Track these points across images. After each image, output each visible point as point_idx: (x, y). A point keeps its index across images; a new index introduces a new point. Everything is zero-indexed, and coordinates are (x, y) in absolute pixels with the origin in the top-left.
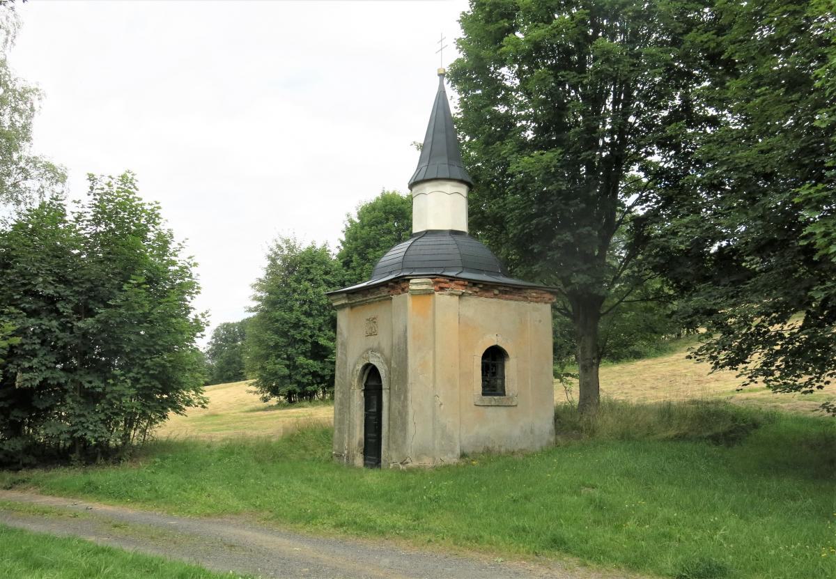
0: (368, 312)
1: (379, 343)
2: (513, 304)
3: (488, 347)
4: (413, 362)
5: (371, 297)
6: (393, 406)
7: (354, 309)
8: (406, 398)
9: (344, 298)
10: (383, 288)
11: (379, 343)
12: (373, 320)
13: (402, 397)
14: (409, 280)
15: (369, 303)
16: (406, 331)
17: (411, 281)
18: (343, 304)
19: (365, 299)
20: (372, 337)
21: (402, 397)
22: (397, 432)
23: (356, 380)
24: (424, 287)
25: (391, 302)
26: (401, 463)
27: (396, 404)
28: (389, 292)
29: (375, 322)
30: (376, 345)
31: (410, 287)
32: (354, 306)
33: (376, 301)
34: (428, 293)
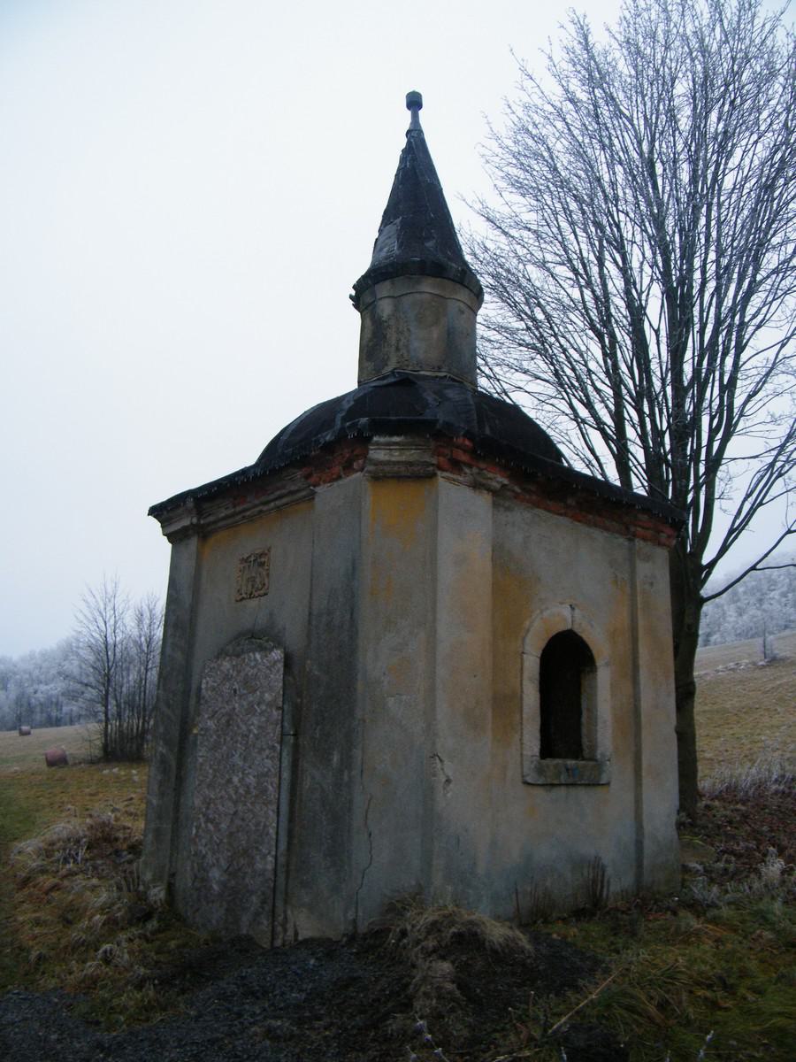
0: (249, 541)
1: (271, 614)
2: (600, 536)
4: (376, 660)
5: (257, 502)
6: (307, 783)
7: (212, 540)
8: (347, 762)
11: (271, 614)
12: (259, 561)
13: (336, 758)
15: (251, 519)
16: (353, 570)
18: (185, 529)
19: (239, 509)
20: (253, 603)
21: (336, 758)
28: (308, 477)
29: (262, 564)
34: (421, 476)
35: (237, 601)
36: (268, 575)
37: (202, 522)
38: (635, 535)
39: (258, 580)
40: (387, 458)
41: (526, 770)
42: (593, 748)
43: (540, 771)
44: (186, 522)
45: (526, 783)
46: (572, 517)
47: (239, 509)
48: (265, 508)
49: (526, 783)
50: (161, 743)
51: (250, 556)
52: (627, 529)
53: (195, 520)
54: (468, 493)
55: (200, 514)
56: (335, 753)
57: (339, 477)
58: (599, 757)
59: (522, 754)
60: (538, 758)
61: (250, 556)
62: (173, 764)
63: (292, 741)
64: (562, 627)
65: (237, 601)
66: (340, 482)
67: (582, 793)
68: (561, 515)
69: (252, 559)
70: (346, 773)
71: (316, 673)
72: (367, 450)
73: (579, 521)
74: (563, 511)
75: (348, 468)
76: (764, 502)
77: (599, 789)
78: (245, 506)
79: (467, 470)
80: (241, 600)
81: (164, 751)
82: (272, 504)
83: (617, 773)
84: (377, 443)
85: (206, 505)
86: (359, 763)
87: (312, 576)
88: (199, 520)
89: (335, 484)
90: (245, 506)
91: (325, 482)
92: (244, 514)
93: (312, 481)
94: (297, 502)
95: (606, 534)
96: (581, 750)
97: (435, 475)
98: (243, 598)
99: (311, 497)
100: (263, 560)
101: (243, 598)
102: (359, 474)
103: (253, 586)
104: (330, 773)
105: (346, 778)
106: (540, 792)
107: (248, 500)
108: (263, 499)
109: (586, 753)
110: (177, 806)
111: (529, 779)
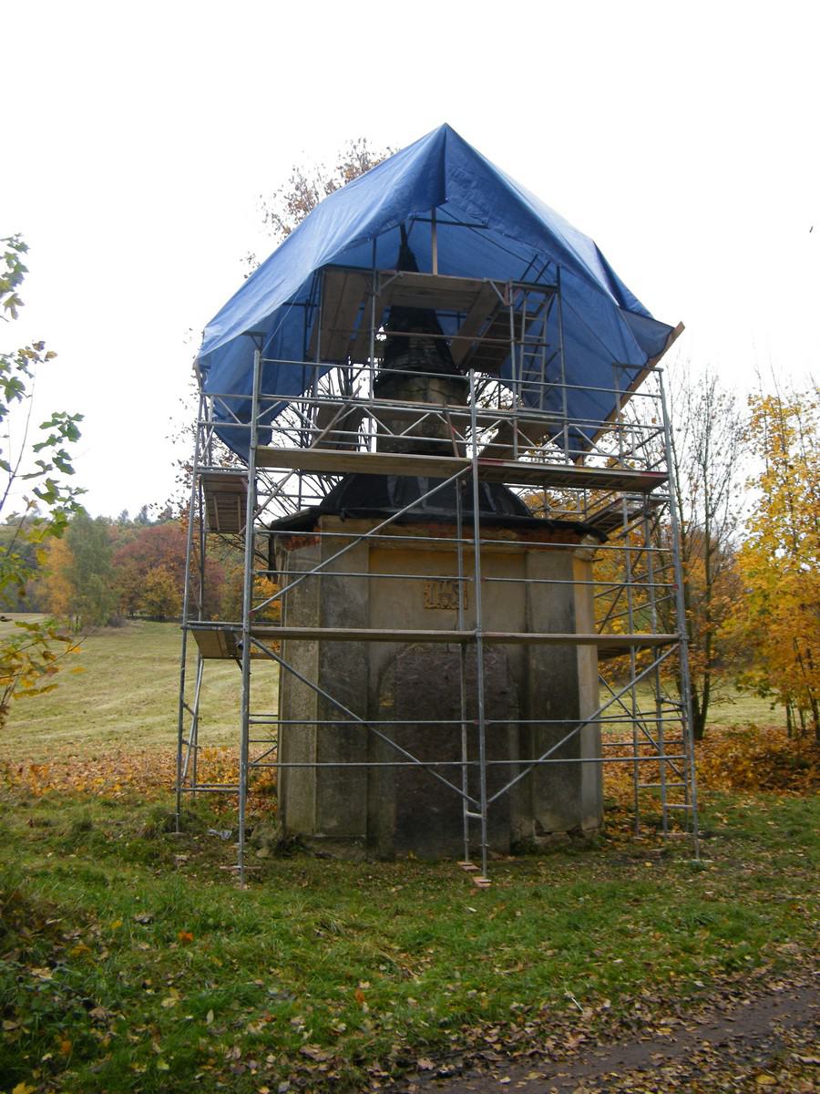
35: (427, 608)
65: (427, 608)
71: (542, 669)
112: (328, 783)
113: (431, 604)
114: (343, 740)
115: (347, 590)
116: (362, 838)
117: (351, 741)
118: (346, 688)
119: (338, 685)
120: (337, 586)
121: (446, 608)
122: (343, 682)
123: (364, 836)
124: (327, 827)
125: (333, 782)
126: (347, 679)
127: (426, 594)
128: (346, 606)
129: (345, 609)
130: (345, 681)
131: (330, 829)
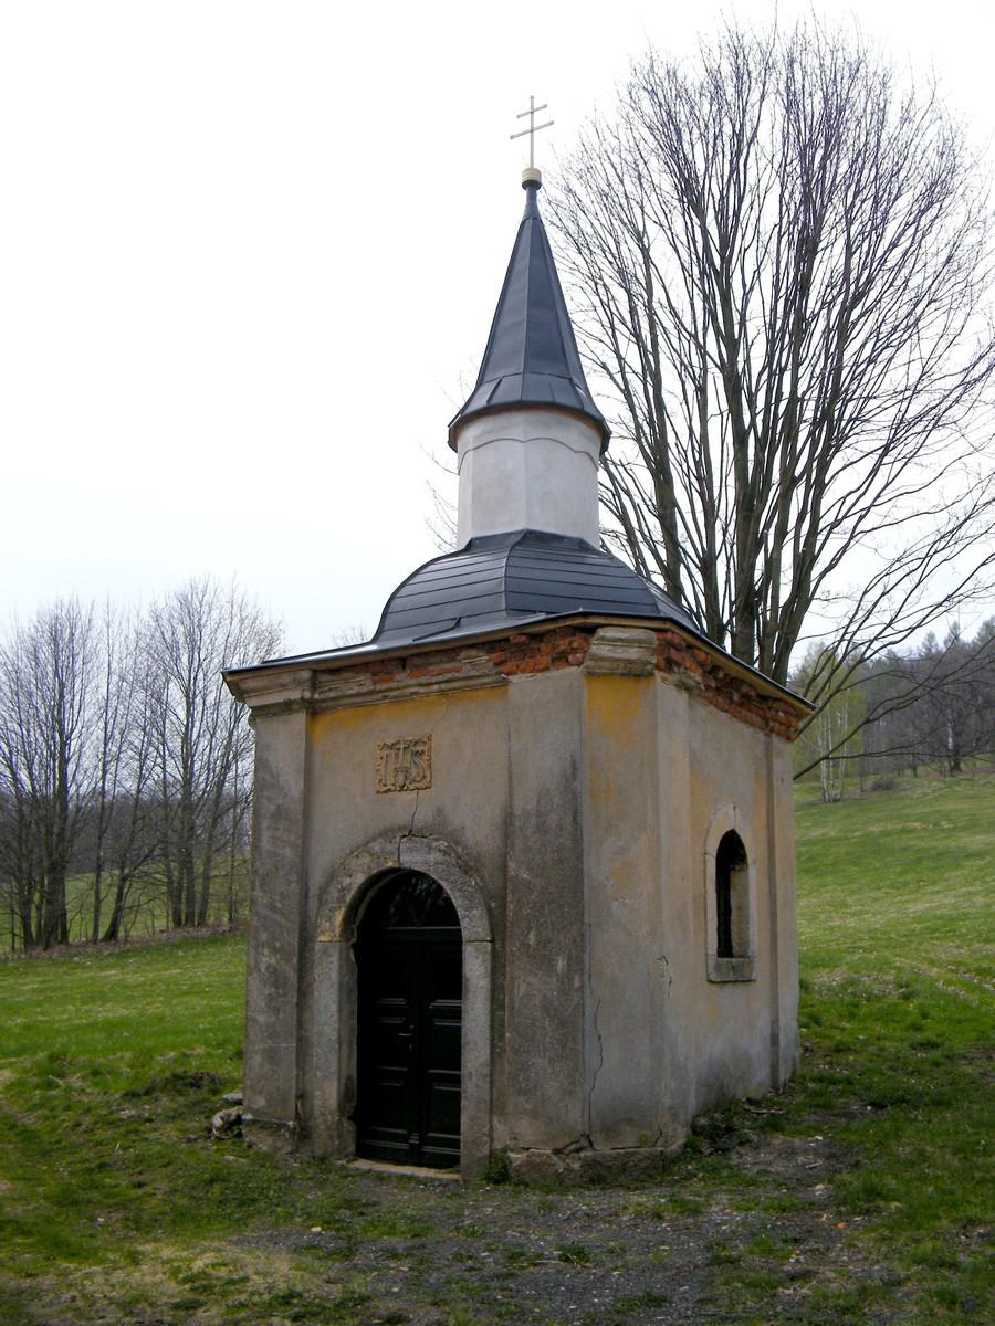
0: (395, 725)
1: (440, 811)
2: (747, 730)
3: (723, 833)
4: (599, 865)
5: (412, 682)
7: (324, 721)
8: (576, 964)
9: (299, 683)
10: (473, 652)
11: (440, 811)
12: (416, 749)
13: (561, 964)
14: (591, 630)
15: (397, 700)
17: (601, 632)
19: (378, 687)
21: (561, 964)
22: (539, 1062)
23: (339, 916)
24: (634, 653)
25: (507, 690)
26: (557, 1152)
27: (527, 985)
30: (424, 816)
31: (594, 649)
32: (323, 711)
33: (427, 694)
35: (378, 792)
36: (430, 766)
37: (317, 696)
38: (772, 730)
39: (414, 771)
40: (610, 654)
41: (710, 971)
42: (745, 943)
43: (718, 968)
44: (295, 695)
45: (711, 982)
46: (732, 713)
47: (378, 687)
48: (422, 690)
49: (711, 982)
50: (266, 952)
51: (399, 742)
52: (767, 725)
53: (307, 695)
54: (674, 690)
55: (314, 686)
56: (560, 958)
57: (547, 669)
58: (750, 954)
59: (706, 954)
60: (715, 957)
61: (399, 742)
62: (293, 976)
63: (489, 948)
64: (729, 829)
65: (378, 792)
66: (547, 674)
67: (740, 989)
68: (726, 711)
69: (402, 746)
70: (577, 978)
71: (525, 876)
72: (589, 644)
73: (735, 717)
74: (727, 708)
75: (562, 658)
76: (843, 687)
77: (752, 984)
78: (392, 685)
79: (676, 669)
80: (385, 792)
81: (273, 961)
82: (436, 687)
83: (760, 970)
84: (603, 638)
85: (324, 678)
86: (588, 967)
87: (510, 773)
88: (312, 693)
89: (539, 675)
90: (392, 685)
91: (523, 671)
92: (385, 694)
93: (505, 668)
94: (473, 688)
95: (751, 729)
96: (731, 947)
97: (651, 674)
98: (389, 790)
99: (505, 683)
100: (420, 748)
101: (389, 790)
102: (574, 669)
103: (406, 778)
104: (555, 979)
105: (577, 983)
106: (714, 988)
107: (398, 677)
108: (423, 680)
109: (736, 949)
110: (300, 1024)
111: (713, 979)
112: (257, 1048)
113: (385, 785)
114: (273, 990)
115: (281, 779)
116: (289, 1126)
117: (281, 991)
118: (277, 917)
119: (270, 913)
120: (272, 776)
121: (402, 789)
122: (274, 909)
123: (291, 1123)
124: (256, 1107)
125: (262, 1046)
126: (279, 905)
127: (378, 771)
128: (280, 801)
129: (279, 805)
130: (275, 907)
131: (258, 1110)
